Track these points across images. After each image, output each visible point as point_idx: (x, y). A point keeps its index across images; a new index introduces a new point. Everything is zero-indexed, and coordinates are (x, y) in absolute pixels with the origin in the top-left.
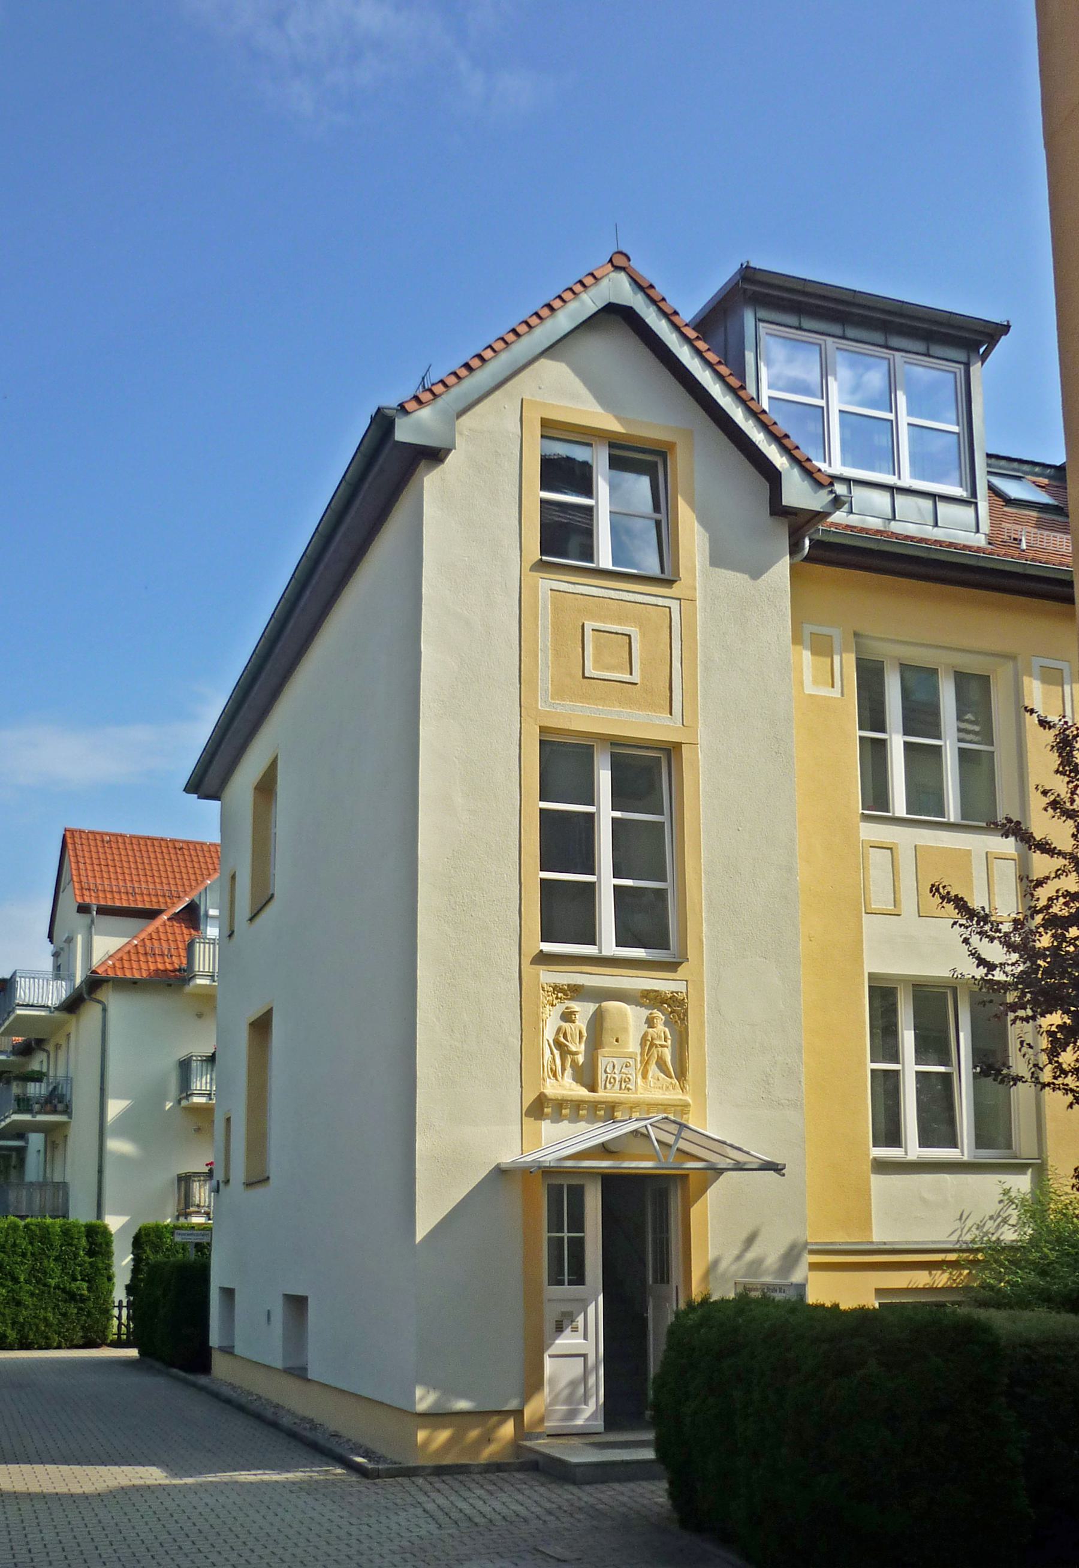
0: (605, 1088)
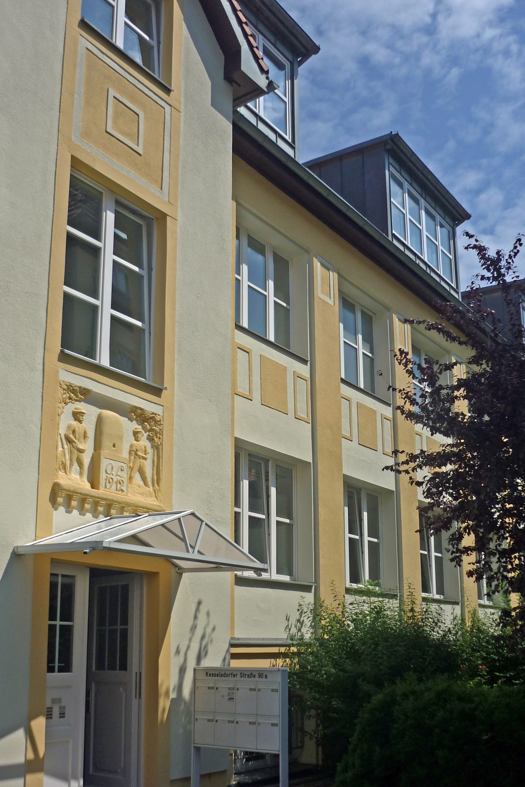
0: (106, 487)
